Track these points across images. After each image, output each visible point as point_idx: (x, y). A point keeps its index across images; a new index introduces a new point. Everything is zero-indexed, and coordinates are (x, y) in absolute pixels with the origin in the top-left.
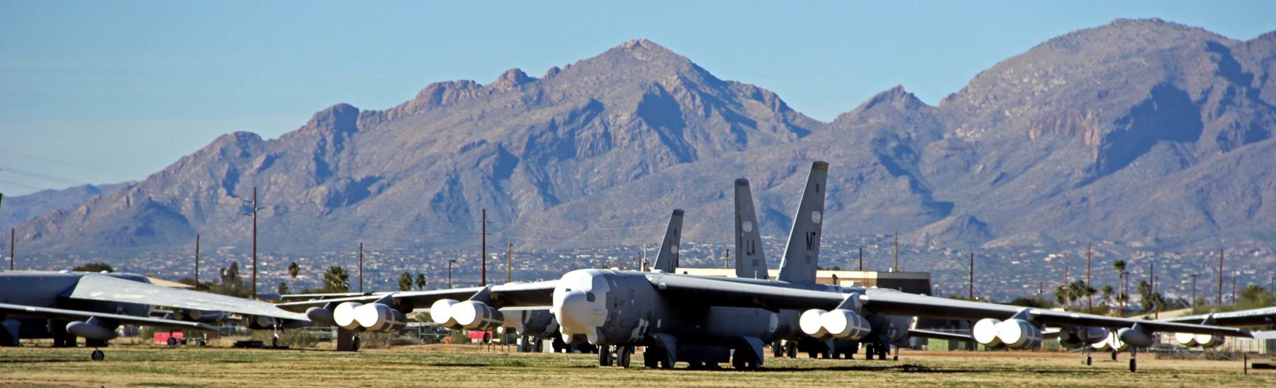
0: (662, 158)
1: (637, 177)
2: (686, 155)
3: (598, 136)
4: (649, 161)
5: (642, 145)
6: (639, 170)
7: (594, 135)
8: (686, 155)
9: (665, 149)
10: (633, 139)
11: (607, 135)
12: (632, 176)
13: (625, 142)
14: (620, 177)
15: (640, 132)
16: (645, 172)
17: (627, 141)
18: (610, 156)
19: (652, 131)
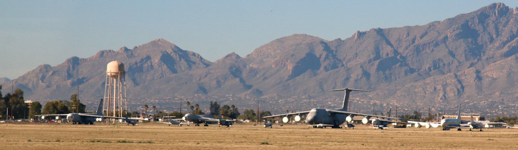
0: (167, 72)
1: (160, 78)
2: (174, 71)
3: (149, 66)
4: (164, 73)
5: (162, 68)
6: (161, 76)
7: (148, 66)
8: (174, 71)
9: (168, 70)
10: (159, 67)
11: (152, 66)
12: (159, 77)
13: (157, 68)
14: (155, 78)
15: (161, 65)
16: (163, 76)
17: (157, 67)
18: (152, 72)
19: (165, 64)
